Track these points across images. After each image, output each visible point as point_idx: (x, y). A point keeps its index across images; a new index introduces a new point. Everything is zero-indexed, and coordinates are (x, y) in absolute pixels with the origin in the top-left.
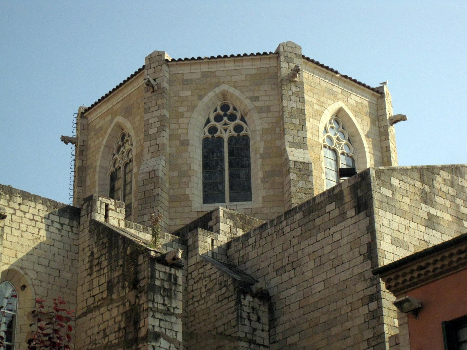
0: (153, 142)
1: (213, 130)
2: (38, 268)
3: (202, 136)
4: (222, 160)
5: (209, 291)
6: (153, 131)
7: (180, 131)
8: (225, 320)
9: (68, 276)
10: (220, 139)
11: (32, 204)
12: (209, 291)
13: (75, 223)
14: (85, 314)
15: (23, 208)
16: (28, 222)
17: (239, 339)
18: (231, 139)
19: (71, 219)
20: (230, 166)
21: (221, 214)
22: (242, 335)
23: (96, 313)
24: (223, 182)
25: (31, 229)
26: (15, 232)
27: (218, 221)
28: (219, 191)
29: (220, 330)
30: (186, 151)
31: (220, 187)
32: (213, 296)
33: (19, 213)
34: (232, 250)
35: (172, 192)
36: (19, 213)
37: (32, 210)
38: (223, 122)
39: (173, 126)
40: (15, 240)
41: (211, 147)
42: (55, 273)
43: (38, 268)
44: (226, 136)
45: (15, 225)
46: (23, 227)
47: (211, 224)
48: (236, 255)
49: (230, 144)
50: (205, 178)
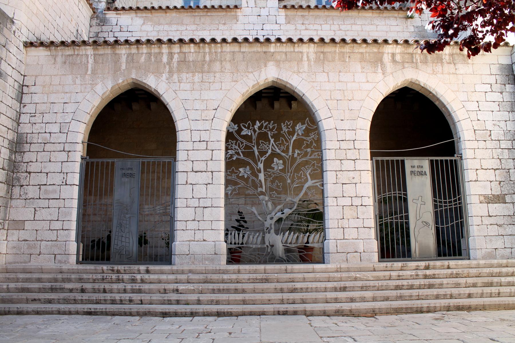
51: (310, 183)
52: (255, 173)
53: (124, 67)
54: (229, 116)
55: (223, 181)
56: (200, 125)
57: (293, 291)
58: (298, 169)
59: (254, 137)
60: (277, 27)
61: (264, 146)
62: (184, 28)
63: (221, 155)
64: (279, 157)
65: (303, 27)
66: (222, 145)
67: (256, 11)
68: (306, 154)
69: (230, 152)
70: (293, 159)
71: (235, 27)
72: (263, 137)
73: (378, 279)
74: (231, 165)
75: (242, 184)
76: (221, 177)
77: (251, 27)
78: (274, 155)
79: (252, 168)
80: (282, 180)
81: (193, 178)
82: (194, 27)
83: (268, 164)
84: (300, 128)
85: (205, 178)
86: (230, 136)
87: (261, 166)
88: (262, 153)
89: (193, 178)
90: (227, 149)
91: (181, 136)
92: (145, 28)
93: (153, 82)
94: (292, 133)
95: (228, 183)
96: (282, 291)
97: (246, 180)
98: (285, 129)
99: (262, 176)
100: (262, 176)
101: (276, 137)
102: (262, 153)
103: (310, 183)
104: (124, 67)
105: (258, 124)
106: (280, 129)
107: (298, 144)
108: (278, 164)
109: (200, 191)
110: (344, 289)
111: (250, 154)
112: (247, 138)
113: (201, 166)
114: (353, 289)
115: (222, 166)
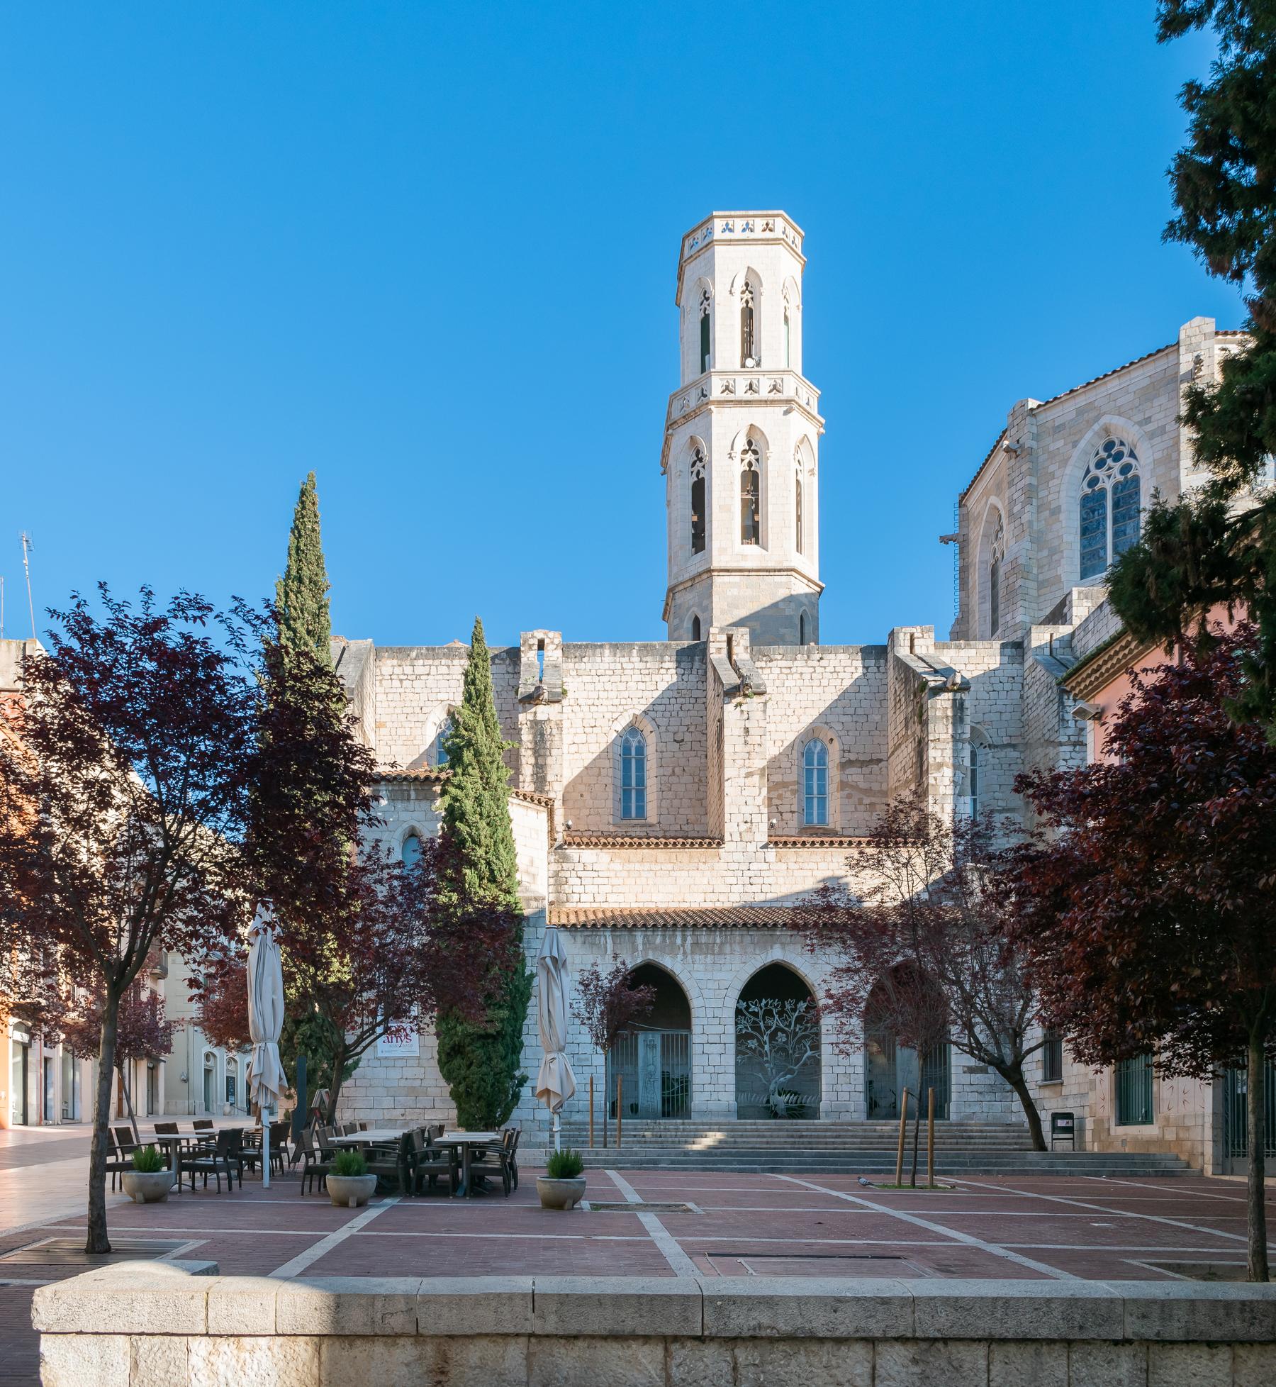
0: (1017, 522)
1: (1094, 482)
2: (843, 719)
3: (1080, 495)
4: (1105, 518)
5: (1039, 696)
6: (1016, 509)
7: (1050, 498)
8: (1050, 726)
9: (877, 718)
10: (1103, 491)
11: (833, 656)
12: (1039, 696)
13: (882, 662)
14: (893, 753)
15: (823, 663)
16: (830, 676)
17: (1061, 744)
18: (1115, 487)
19: (877, 659)
20: (1115, 521)
21: (1075, 596)
22: (1064, 739)
23: (899, 751)
24: (1104, 548)
25: (833, 682)
26: (817, 690)
27: (1071, 607)
28: (1100, 558)
29: (1047, 737)
30: (1058, 520)
31: (1102, 553)
32: (1042, 701)
33: (818, 670)
34: (1075, 641)
35: (1041, 577)
36: (819, 670)
37: (832, 663)
38: (1106, 467)
39: (1041, 494)
40: (816, 697)
41: (1091, 504)
42: (863, 719)
43: (843, 719)
44: (1108, 486)
45: (816, 683)
46: (824, 682)
47: (1066, 610)
48: (1079, 646)
49: (1114, 493)
50: (1083, 547)
51: (809, 1053)
52: (761, 1045)
53: (640, 948)
54: (737, 994)
55: (733, 1051)
56: (713, 1003)
57: (801, 1137)
58: (799, 1042)
59: (761, 1013)
60: (765, 866)
61: (769, 1021)
62: (658, 867)
63: (731, 1029)
64: (783, 1031)
65: (797, 866)
66: (732, 1021)
67: (741, 846)
68: (806, 1029)
69: (740, 1027)
70: (796, 1033)
71: (717, 866)
72: (768, 1013)
73: (865, 1131)
74: (741, 1038)
75: (750, 1053)
76: (732, 1048)
77: (735, 866)
78: (778, 1029)
79: (759, 1041)
80: (784, 1050)
81: (708, 1048)
82: (670, 866)
83: (773, 1036)
84: (802, 1006)
85: (719, 1048)
86: (738, 1012)
87: (766, 1038)
88: (768, 1028)
89: (708, 1048)
90: (736, 1024)
91: (694, 1013)
92: (612, 866)
93: (670, 962)
94: (794, 1010)
95: (738, 1053)
96: (792, 1137)
97: (754, 1051)
98: (788, 1007)
99: (767, 1047)
100: (767, 1047)
101: (780, 1014)
102: (768, 1028)
103: (809, 1053)
104: (640, 948)
105: (764, 1002)
106: (783, 1006)
107: (800, 1020)
108: (781, 1038)
109: (715, 1060)
110: (839, 1137)
111: (757, 1029)
112: (755, 1014)
113: (716, 1039)
114: (845, 1137)
115: (732, 1039)
